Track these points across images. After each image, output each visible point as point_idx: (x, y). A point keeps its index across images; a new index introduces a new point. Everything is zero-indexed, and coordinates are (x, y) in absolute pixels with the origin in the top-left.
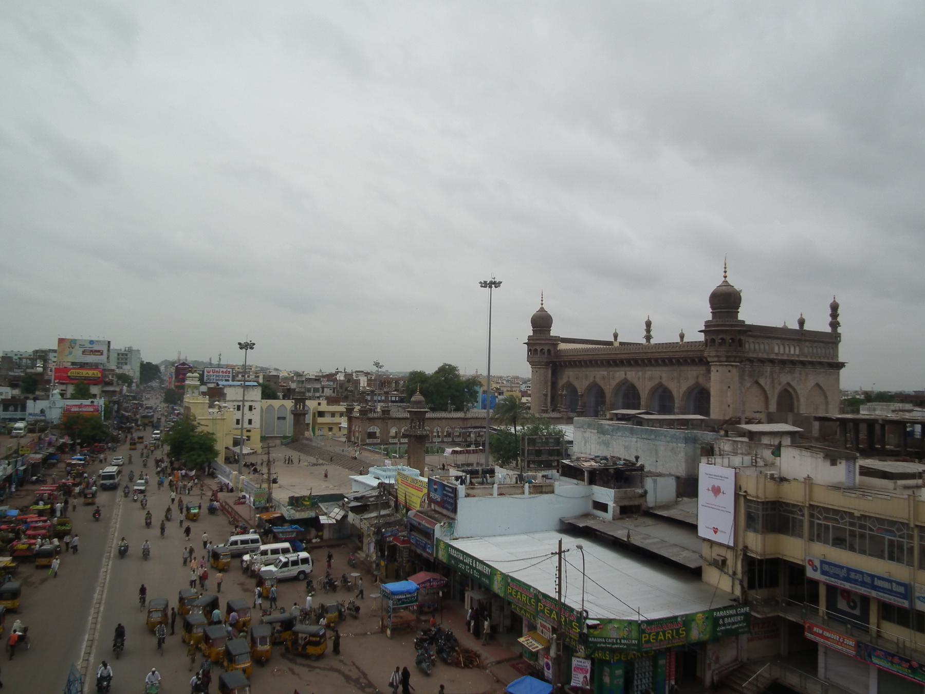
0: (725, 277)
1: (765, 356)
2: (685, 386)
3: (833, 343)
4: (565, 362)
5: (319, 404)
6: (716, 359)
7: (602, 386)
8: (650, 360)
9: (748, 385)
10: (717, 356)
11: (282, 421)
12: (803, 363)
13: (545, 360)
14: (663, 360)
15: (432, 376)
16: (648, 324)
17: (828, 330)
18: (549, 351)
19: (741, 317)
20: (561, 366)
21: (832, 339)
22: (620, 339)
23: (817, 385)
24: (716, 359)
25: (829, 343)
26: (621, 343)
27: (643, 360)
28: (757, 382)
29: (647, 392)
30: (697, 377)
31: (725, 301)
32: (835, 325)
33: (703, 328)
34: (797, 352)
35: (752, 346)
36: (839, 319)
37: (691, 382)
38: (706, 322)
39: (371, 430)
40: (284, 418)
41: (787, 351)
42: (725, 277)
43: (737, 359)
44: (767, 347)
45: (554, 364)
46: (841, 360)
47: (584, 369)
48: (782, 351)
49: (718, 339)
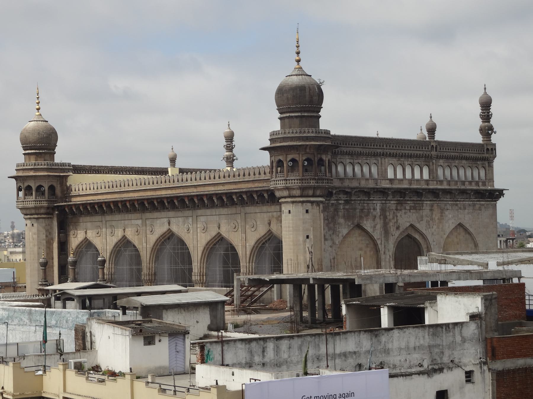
0: (298, 61)
1: (371, 184)
2: (253, 237)
3: (484, 159)
4: (77, 206)
6: (286, 193)
7: (136, 243)
8: (200, 197)
9: (345, 231)
10: (287, 188)
12: (435, 194)
13: (45, 204)
14: (219, 196)
16: (230, 138)
17: (478, 139)
18: (52, 188)
19: (324, 125)
20: (73, 213)
21: (482, 154)
22: (180, 163)
23: (460, 225)
24: (286, 193)
25: (476, 159)
26: (182, 171)
27: (191, 198)
28: (359, 226)
29: (200, 249)
30: (269, 224)
31: (301, 101)
32: (487, 131)
33: (268, 144)
34: (426, 176)
35: (349, 169)
36: (493, 121)
37: (262, 231)
38: (273, 134)
41: (408, 176)
42: (298, 61)
43: (318, 192)
44: (374, 170)
45: (61, 209)
46: (497, 185)
47: (108, 218)
48: (400, 176)
49: (286, 159)
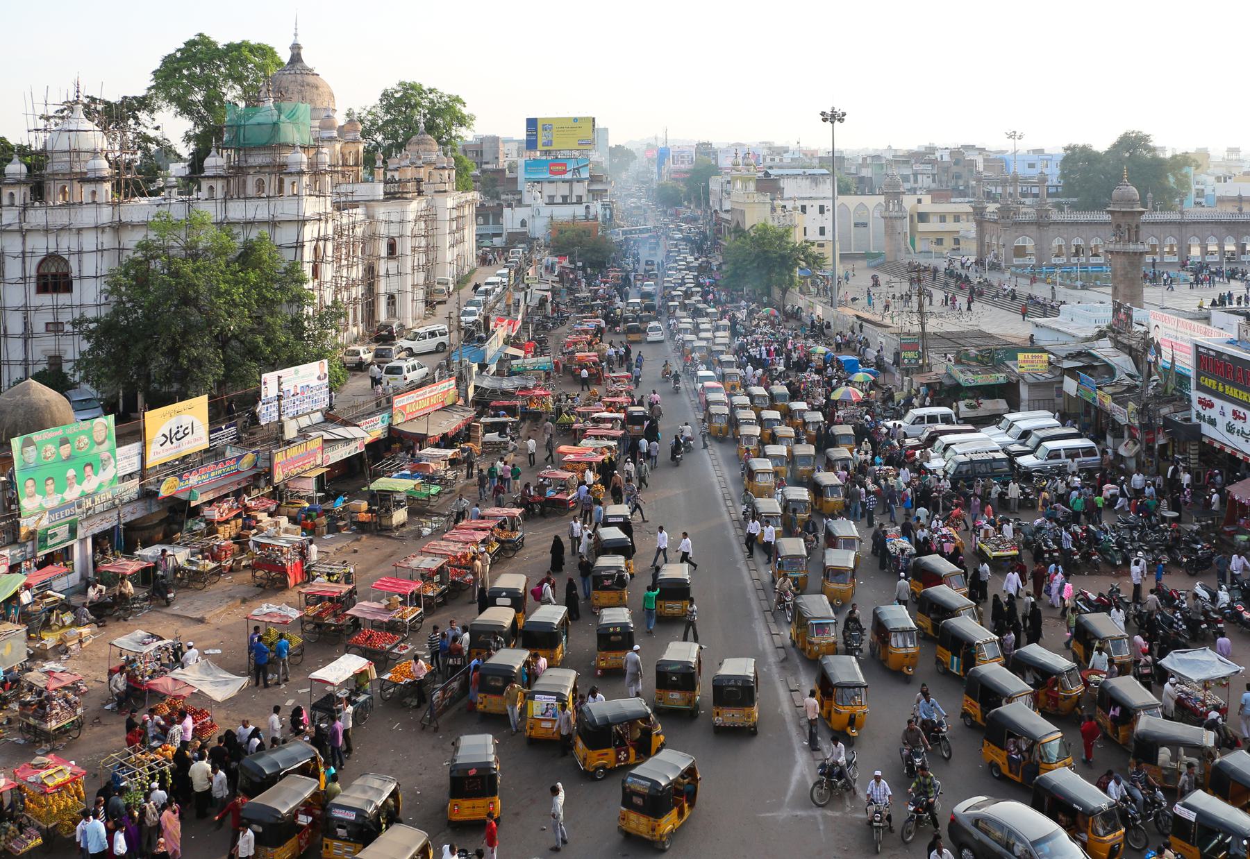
5: (919, 201)
11: (862, 229)
15: (1098, 154)
39: (1019, 242)
40: (865, 225)
